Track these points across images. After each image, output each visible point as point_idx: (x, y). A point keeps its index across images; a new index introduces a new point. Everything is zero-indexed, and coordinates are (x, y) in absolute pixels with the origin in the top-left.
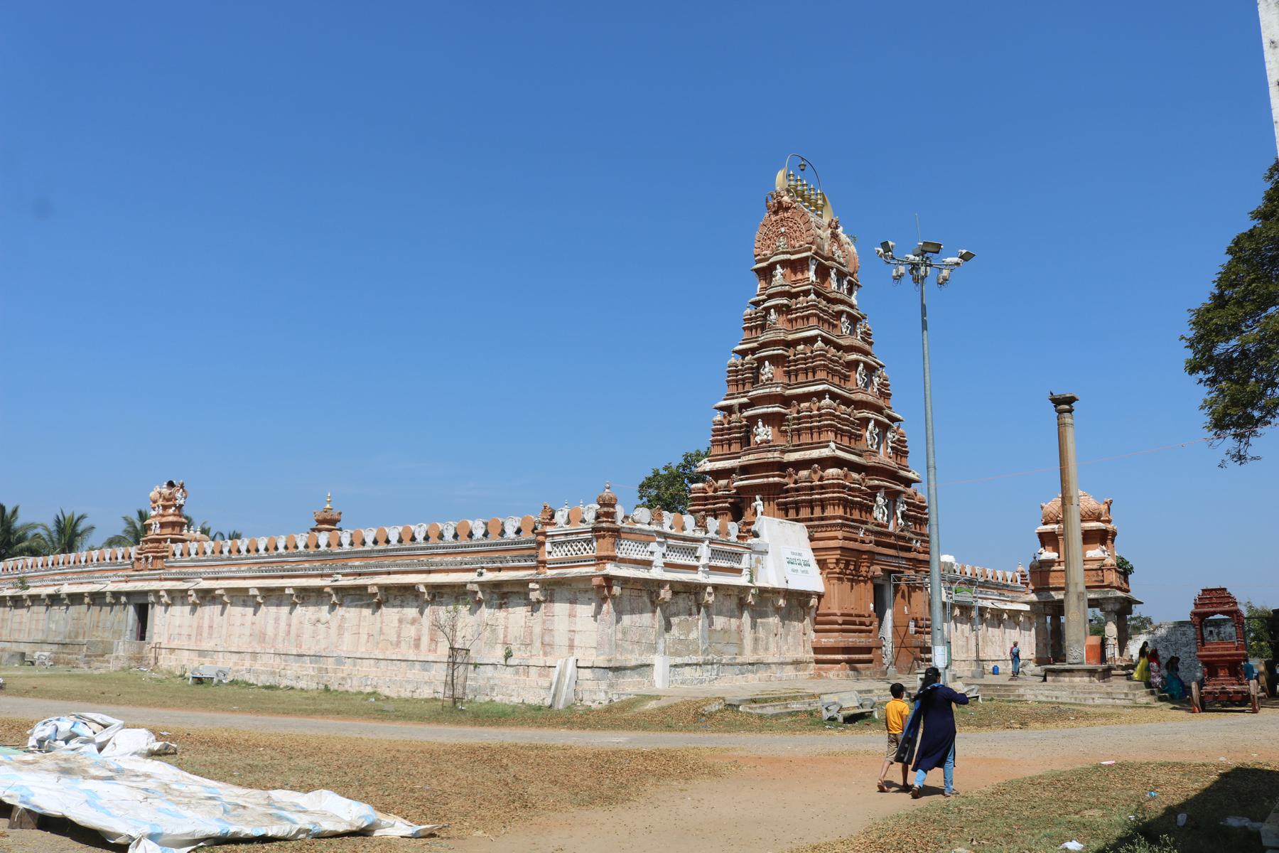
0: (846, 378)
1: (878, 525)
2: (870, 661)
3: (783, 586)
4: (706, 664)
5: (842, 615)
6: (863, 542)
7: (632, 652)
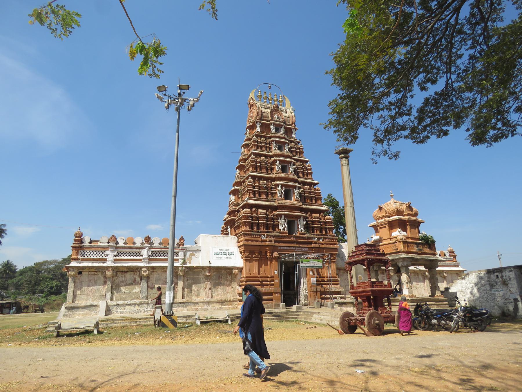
0: (272, 169)
1: (280, 233)
2: (272, 300)
4: (141, 303)
5: (247, 277)
6: (266, 241)
7: (87, 299)
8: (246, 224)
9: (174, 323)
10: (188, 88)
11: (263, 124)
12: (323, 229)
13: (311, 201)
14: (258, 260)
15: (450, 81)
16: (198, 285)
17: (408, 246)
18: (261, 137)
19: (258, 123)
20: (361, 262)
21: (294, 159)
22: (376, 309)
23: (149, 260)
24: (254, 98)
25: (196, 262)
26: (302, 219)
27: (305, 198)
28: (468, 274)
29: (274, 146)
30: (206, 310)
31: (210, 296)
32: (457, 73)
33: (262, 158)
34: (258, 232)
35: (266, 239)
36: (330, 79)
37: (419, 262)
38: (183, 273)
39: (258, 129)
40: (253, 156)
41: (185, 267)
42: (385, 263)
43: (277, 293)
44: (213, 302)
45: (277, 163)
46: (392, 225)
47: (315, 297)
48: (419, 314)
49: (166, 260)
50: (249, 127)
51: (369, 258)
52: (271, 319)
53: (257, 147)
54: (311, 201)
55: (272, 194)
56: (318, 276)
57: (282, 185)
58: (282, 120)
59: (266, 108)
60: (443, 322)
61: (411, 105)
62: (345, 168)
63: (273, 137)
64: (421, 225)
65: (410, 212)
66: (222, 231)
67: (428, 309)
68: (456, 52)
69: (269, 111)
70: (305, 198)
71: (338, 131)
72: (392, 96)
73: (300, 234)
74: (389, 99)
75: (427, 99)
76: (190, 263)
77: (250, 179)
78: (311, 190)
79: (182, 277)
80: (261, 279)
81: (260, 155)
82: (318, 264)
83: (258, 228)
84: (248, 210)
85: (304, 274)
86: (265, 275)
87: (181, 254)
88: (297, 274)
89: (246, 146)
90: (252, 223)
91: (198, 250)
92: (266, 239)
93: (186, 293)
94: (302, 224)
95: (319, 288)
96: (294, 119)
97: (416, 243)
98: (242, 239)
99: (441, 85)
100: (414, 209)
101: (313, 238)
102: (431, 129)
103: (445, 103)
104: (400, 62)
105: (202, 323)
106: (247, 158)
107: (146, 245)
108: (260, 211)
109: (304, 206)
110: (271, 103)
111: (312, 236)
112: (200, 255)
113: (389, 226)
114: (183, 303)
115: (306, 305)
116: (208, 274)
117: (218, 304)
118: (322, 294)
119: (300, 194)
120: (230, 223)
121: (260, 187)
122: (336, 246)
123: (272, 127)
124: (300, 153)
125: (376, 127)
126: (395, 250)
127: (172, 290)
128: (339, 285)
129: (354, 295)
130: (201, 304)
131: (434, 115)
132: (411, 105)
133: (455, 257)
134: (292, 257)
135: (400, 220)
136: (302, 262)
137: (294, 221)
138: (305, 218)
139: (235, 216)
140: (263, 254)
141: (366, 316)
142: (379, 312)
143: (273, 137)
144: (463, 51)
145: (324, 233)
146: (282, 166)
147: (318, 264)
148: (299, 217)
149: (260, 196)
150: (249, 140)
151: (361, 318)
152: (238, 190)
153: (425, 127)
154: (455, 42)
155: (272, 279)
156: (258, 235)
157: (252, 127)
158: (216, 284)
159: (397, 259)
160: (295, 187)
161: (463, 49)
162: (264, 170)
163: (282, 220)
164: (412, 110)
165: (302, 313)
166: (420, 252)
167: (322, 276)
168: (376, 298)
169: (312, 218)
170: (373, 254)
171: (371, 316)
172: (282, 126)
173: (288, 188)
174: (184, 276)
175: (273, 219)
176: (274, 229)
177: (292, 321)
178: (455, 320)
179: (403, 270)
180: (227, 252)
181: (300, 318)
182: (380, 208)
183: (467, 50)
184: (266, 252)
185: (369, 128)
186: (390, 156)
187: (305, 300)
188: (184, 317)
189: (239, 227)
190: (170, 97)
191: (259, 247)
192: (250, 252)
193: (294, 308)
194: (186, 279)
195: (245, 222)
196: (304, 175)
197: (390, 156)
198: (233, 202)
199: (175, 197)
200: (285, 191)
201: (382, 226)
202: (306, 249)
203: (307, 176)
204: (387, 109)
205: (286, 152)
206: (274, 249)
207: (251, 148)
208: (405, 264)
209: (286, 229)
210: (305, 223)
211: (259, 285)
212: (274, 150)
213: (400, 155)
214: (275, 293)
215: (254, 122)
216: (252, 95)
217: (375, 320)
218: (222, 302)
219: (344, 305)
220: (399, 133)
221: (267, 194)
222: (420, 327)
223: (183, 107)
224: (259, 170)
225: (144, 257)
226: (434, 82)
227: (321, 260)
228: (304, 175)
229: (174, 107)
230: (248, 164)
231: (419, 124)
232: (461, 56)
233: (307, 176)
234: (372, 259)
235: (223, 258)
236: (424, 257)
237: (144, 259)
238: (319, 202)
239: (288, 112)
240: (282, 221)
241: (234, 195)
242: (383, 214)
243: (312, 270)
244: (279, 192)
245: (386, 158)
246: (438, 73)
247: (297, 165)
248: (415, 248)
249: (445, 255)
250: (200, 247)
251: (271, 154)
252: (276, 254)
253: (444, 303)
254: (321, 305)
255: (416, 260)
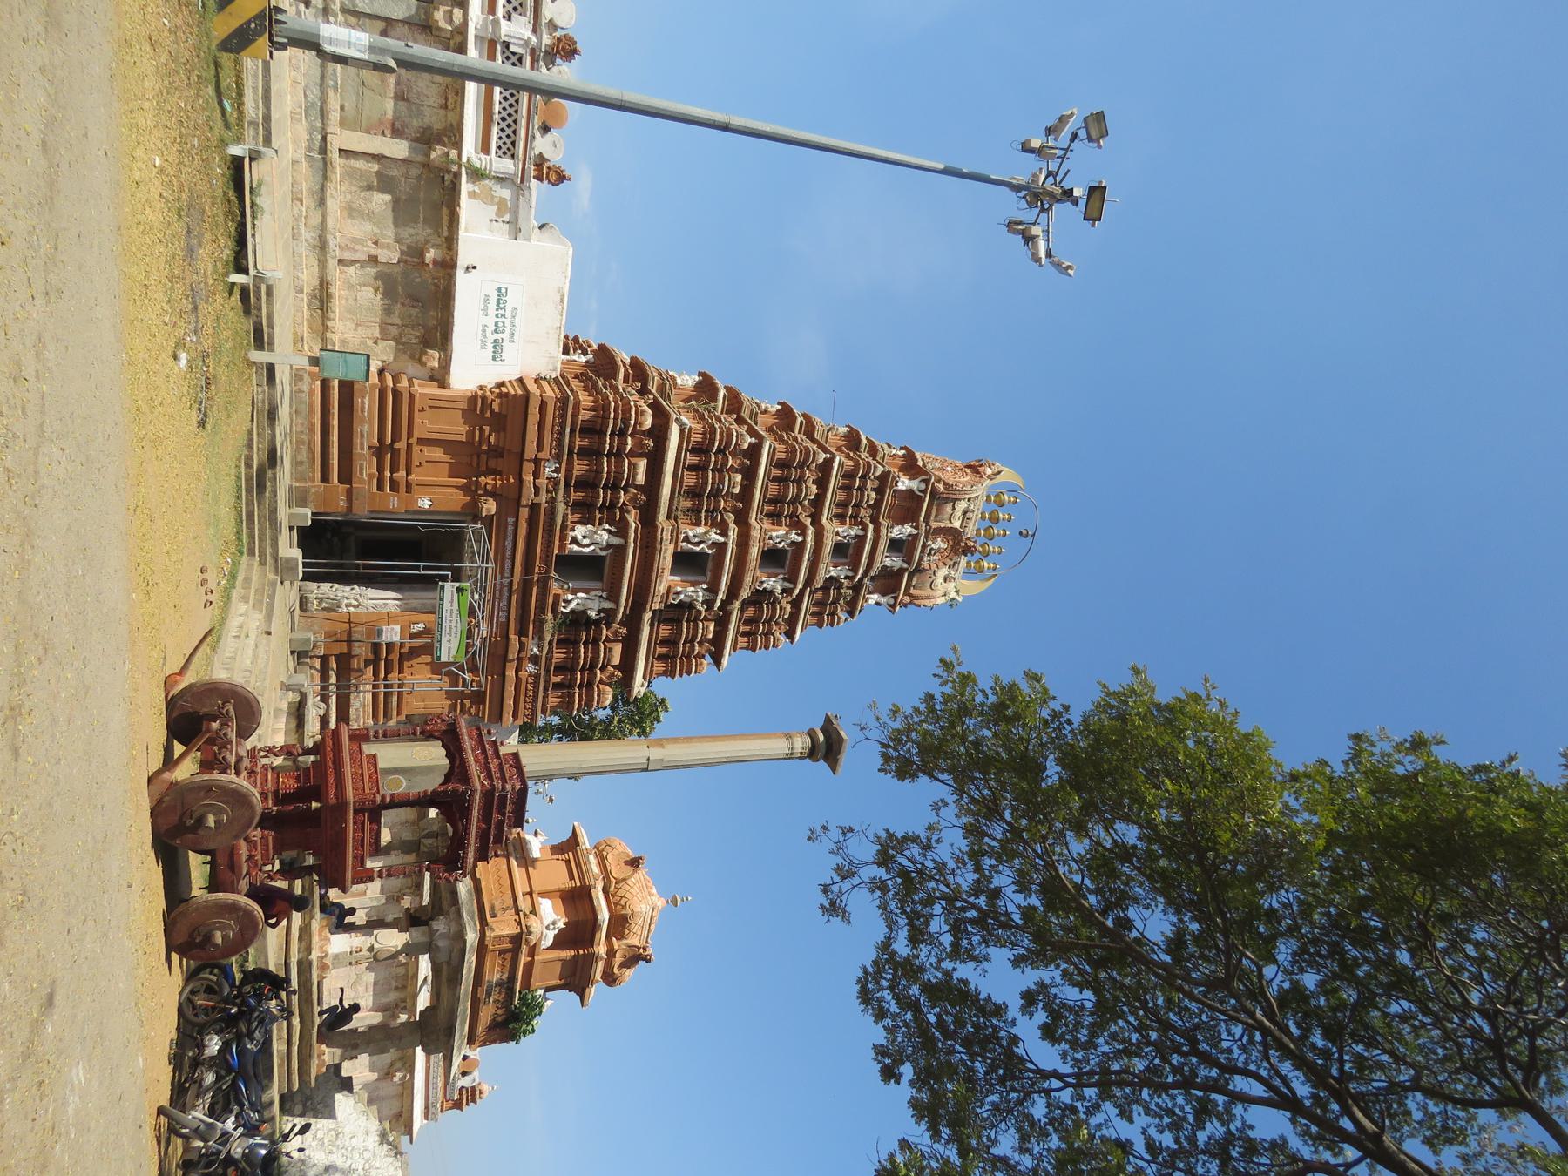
0: (775, 517)
1: (564, 528)
2: (325, 478)
3: (464, 257)
5: (411, 396)
6: (536, 475)
8: (601, 409)
9: (239, 41)
10: (1092, 216)
11: (920, 501)
12: (570, 677)
13: (663, 643)
14: (470, 442)
15: (1055, 1083)
16: (390, 214)
17: (502, 952)
18: (880, 491)
19: (923, 486)
20: (457, 769)
21: (802, 592)
22: (266, 821)
23: (492, 44)
24: (999, 478)
25: (475, 217)
26: (608, 605)
27: (675, 622)
28: (398, 1153)
29: (848, 531)
30: (295, 236)
31: (347, 255)
32: (1078, 1104)
33: (814, 489)
34: (570, 452)
35: (544, 478)
36: (1119, 680)
37: (444, 989)
38: (437, 163)
39: (904, 483)
40: (822, 457)
41: (457, 175)
42: (451, 860)
43: (350, 500)
44: (323, 264)
45: (794, 537)
46: (576, 899)
47: (328, 635)
48: (248, 988)
49: (485, 149)
50: (910, 458)
51: (471, 801)
52: (249, 458)
53: (850, 476)
54: (663, 643)
55: (695, 511)
56: (405, 650)
57: (725, 544)
58: (925, 565)
59: (965, 513)
60: (210, 1078)
61: (987, 959)
62: (778, 746)
63: (877, 531)
64: (573, 997)
65: (618, 960)
66: (576, 339)
67: (266, 1020)
68: (1137, 1102)
69: (957, 524)
70: (675, 622)
71: (931, 710)
72: (1019, 899)
73: (557, 597)
74: (1009, 891)
75: (999, 1010)
76: (472, 195)
77: (749, 440)
78: (701, 643)
79: (419, 158)
80: (401, 445)
81: (822, 483)
82: (449, 648)
83: (583, 453)
84: (648, 423)
85: (415, 603)
86: (415, 462)
87: (506, 166)
88: (417, 568)
89: (852, 440)
90: (602, 433)
91: (516, 233)
92: (544, 478)
93: (360, 164)
94: (590, 604)
95: (362, 651)
96: (926, 602)
97: (512, 978)
98: (549, 393)
99: (1045, 1055)
100: (629, 973)
101: (541, 639)
102: (906, 1025)
103: (980, 1067)
104: (1127, 924)
105: (237, 165)
106: (814, 441)
107: (547, 40)
108: (642, 465)
109: (648, 616)
110: (978, 534)
111: (547, 637)
112: (500, 234)
113: (573, 889)
114: (323, 150)
115: (303, 602)
116: (430, 256)
117: (316, 282)
118: (340, 660)
119: (688, 606)
120: (604, 362)
121: (720, 471)
122: (508, 716)
123: (908, 529)
124: (818, 615)
125: (938, 841)
126: (493, 907)
127: (375, 58)
128: (370, 722)
129: (330, 742)
130: (316, 219)
131: (947, 1035)
132: (987, 959)
133: (458, 1105)
134: (479, 558)
135: (594, 925)
136: (460, 590)
137: (601, 579)
138: (608, 616)
139: (626, 380)
140: (492, 463)
141: (242, 782)
142: (256, 834)
143: (877, 531)
144: (1141, 1120)
145: (558, 679)
146: (783, 551)
147: (449, 648)
148: (614, 596)
149: (692, 468)
150: (873, 450)
151: (233, 760)
152: (715, 400)
153: (914, 1006)
154: (1173, 1098)
155: (403, 488)
156: (560, 447)
157: (910, 466)
158: (390, 285)
159: (460, 916)
160: (713, 589)
161: (1149, 1119)
162: (773, 489)
163: (606, 536)
164: (971, 964)
165: (271, 576)
166: (482, 993)
167: (406, 664)
168: (311, 826)
169: (607, 639)
170: (486, 816)
171: (238, 798)
172: (909, 562)
173: (710, 565)
174: (427, 165)
175: (613, 505)
176: (577, 506)
177: (238, 533)
178: (210, 1126)
179: (418, 934)
180: (506, 336)
181: (250, 567)
182: (635, 863)
183: (1144, 1132)
184: (500, 474)
185: (933, 819)
186: (835, 888)
187: (321, 601)
188: (267, 119)
189: (592, 388)
190: (1062, 158)
191: (517, 449)
192: (501, 413)
193: (291, 550)
194: (414, 172)
195: (606, 408)
196: (748, 622)
197: (835, 888)
198: (673, 379)
199: (725, 128)
200: (703, 554)
201: (575, 867)
202: (503, 614)
203: (744, 634)
204: (978, 881)
205: (829, 569)
206: (510, 500)
207: (848, 456)
208: (441, 943)
209: (575, 548)
210: (592, 614)
211: (381, 438)
212: (836, 532)
213: (836, 921)
214: (349, 493)
215: (926, 473)
216: (1008, 475)
217: (220, 811)
218: (322, 298)
219: (293, 724)
220: (902, 921)
221: (695, 493)
222: (192, 992)
223: (1023, 204)
224: (776, 472)
225: (503, 23)
226: (1049, 1033)
227: (463, 660)
228: (748, 622)
229: (1026, 169)
230: (795, 439)
231: (927, 988)
232: (1125, 1114)
233: (744, 634)
234: (466, 813)
235: (485, 320)
236: (465, 1006)
237: (496, 23)
238: (659, 667)
239: (948, 585)
240: (603, 537)
241: (698, 385)
242: (616, 870)
243: (427, 632)
244: (702, 536)
245: (828, 875)
246: (1074, 1044)
247: (784, 602)
248: (496, 976)
249: (464, 1074)
250: (528, 239)
251: (824, 521)
252: (489, 507)
253: (295, 1077)
254: (300, 655)
255: (455, 980)
